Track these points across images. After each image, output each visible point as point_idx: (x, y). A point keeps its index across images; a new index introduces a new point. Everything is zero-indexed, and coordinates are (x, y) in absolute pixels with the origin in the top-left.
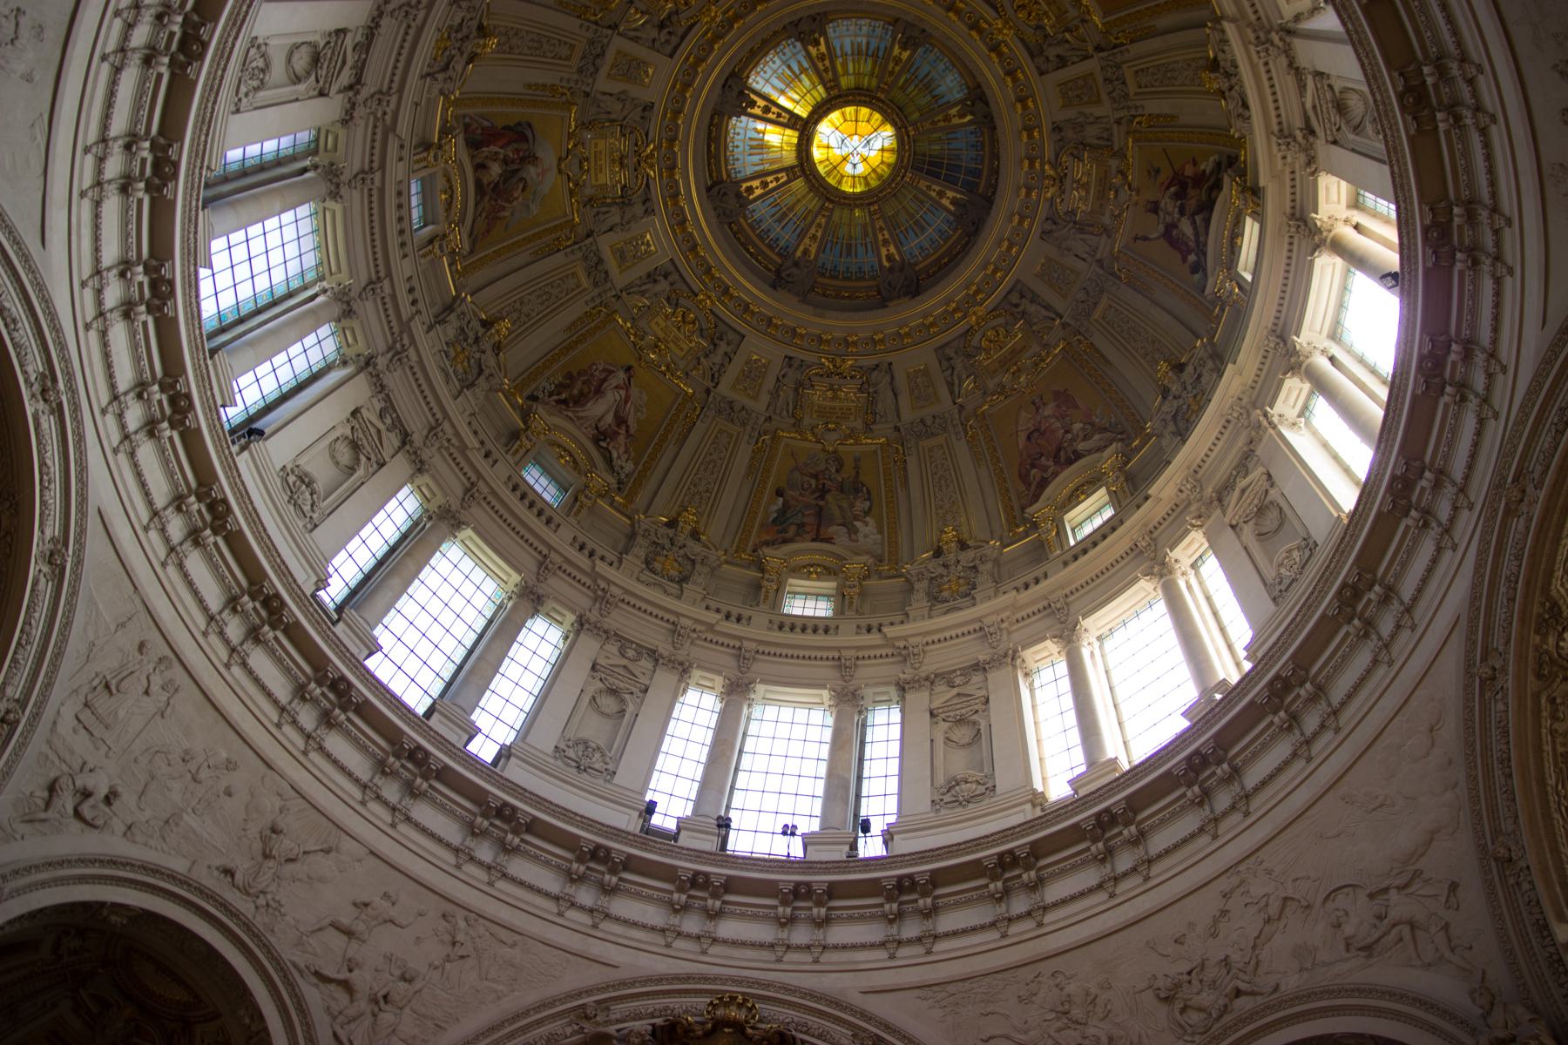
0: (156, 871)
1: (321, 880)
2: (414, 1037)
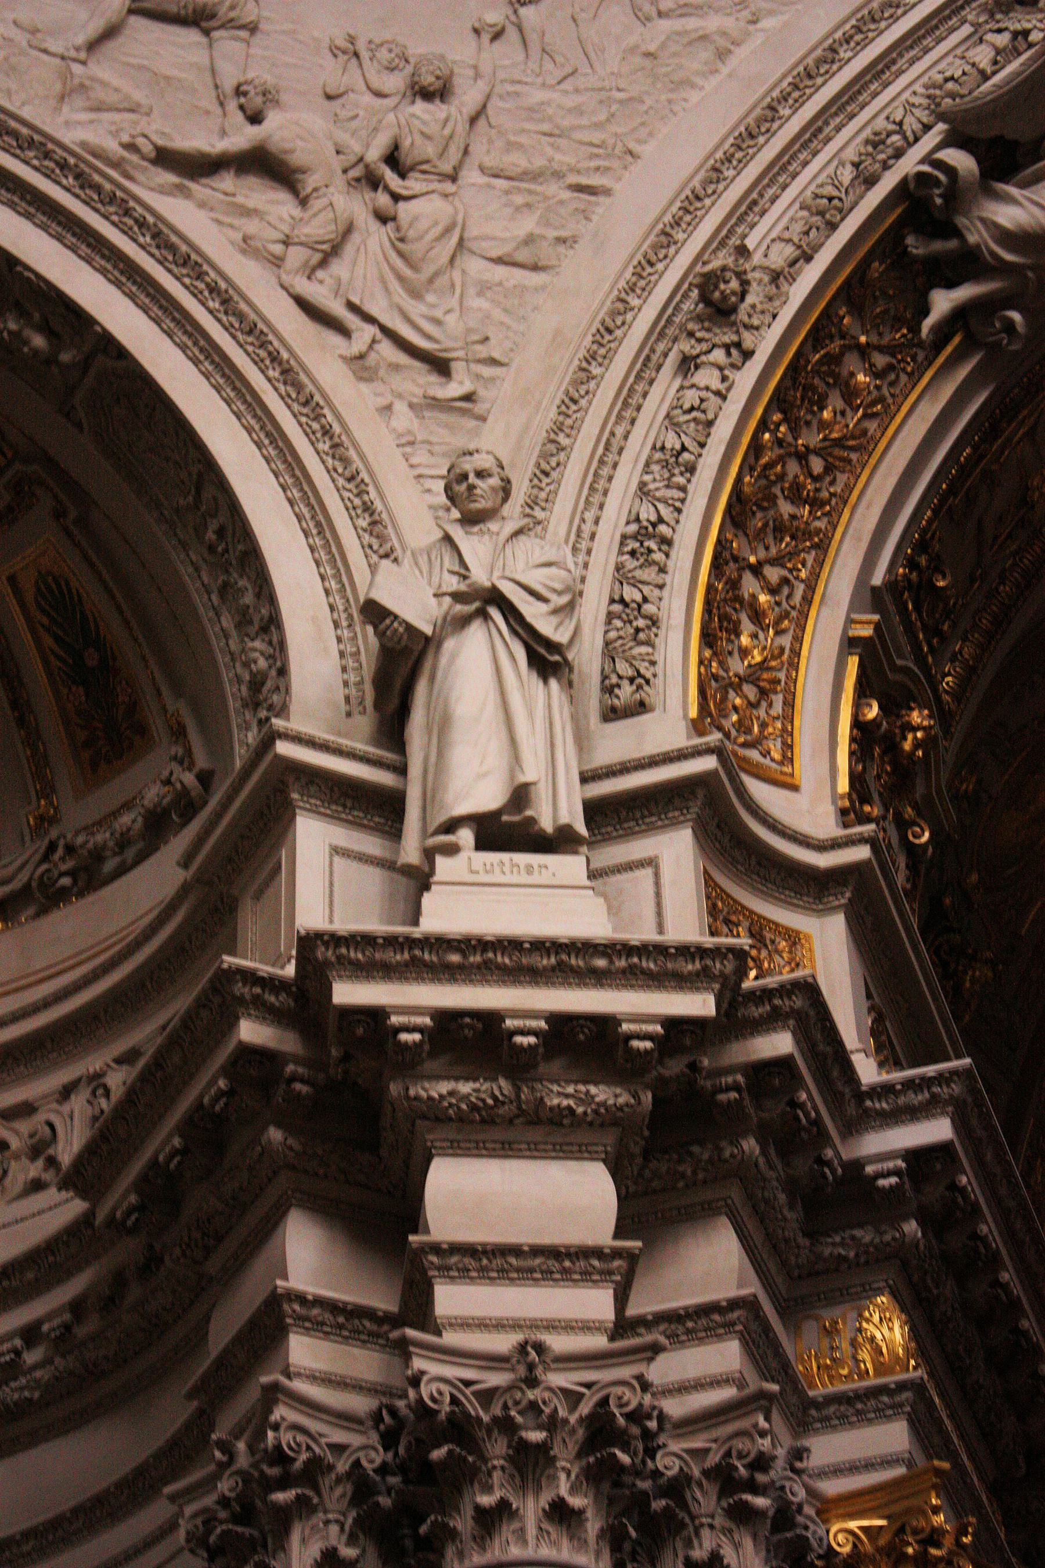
2: (529, 240)
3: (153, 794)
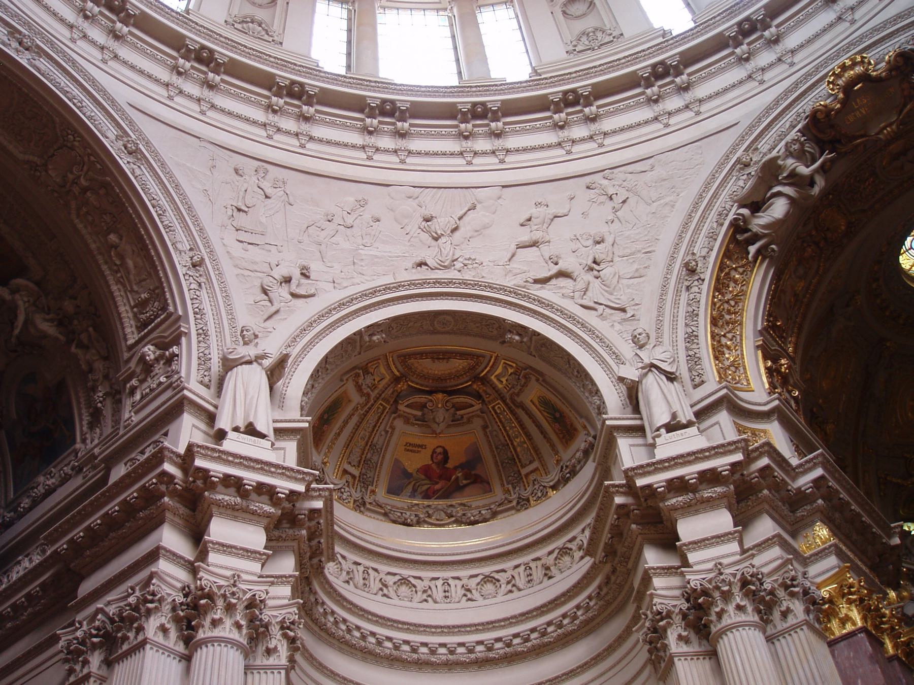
0: (374, 292)
1: (485, 227)
2: (637, 270)
3: (583, 446)
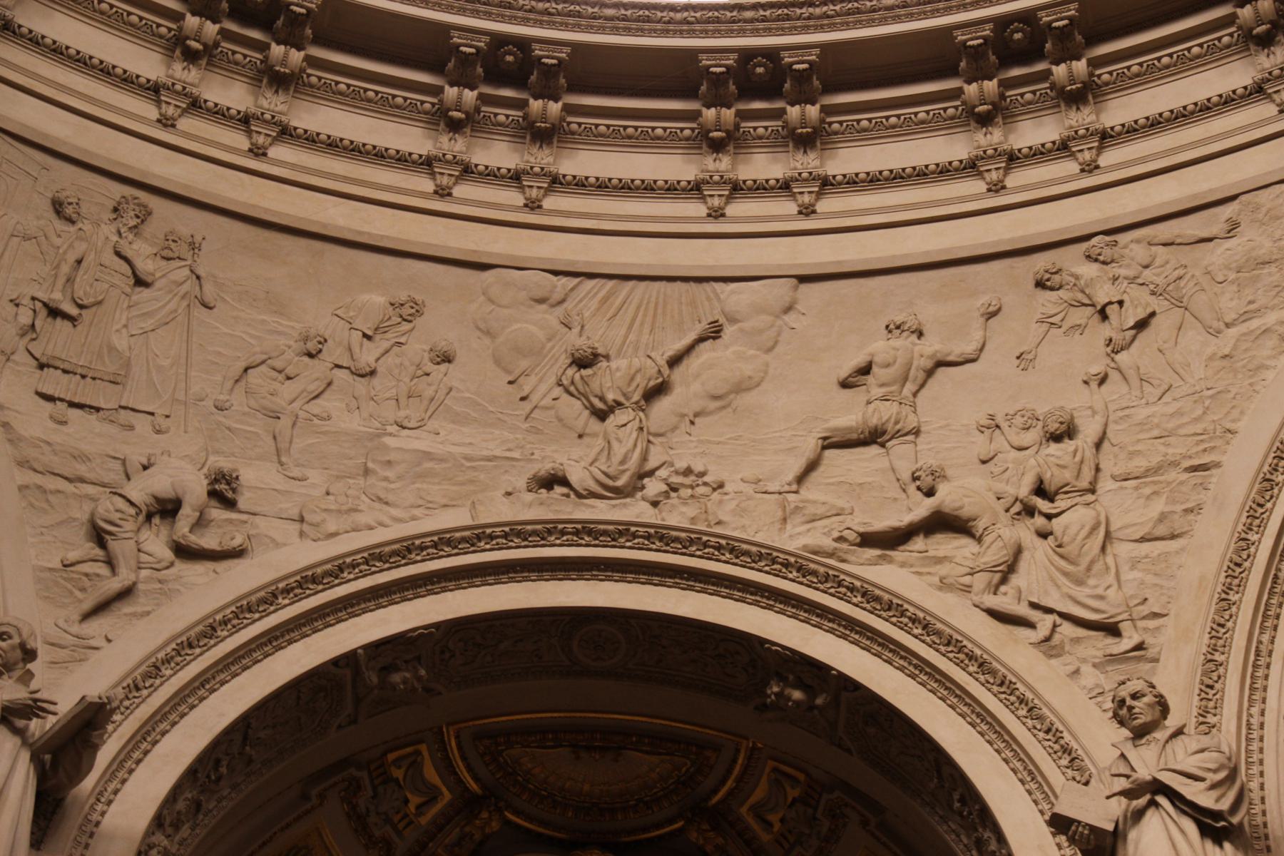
0: (407, 549)
1: (740, 388)
2: (1162, 518)
